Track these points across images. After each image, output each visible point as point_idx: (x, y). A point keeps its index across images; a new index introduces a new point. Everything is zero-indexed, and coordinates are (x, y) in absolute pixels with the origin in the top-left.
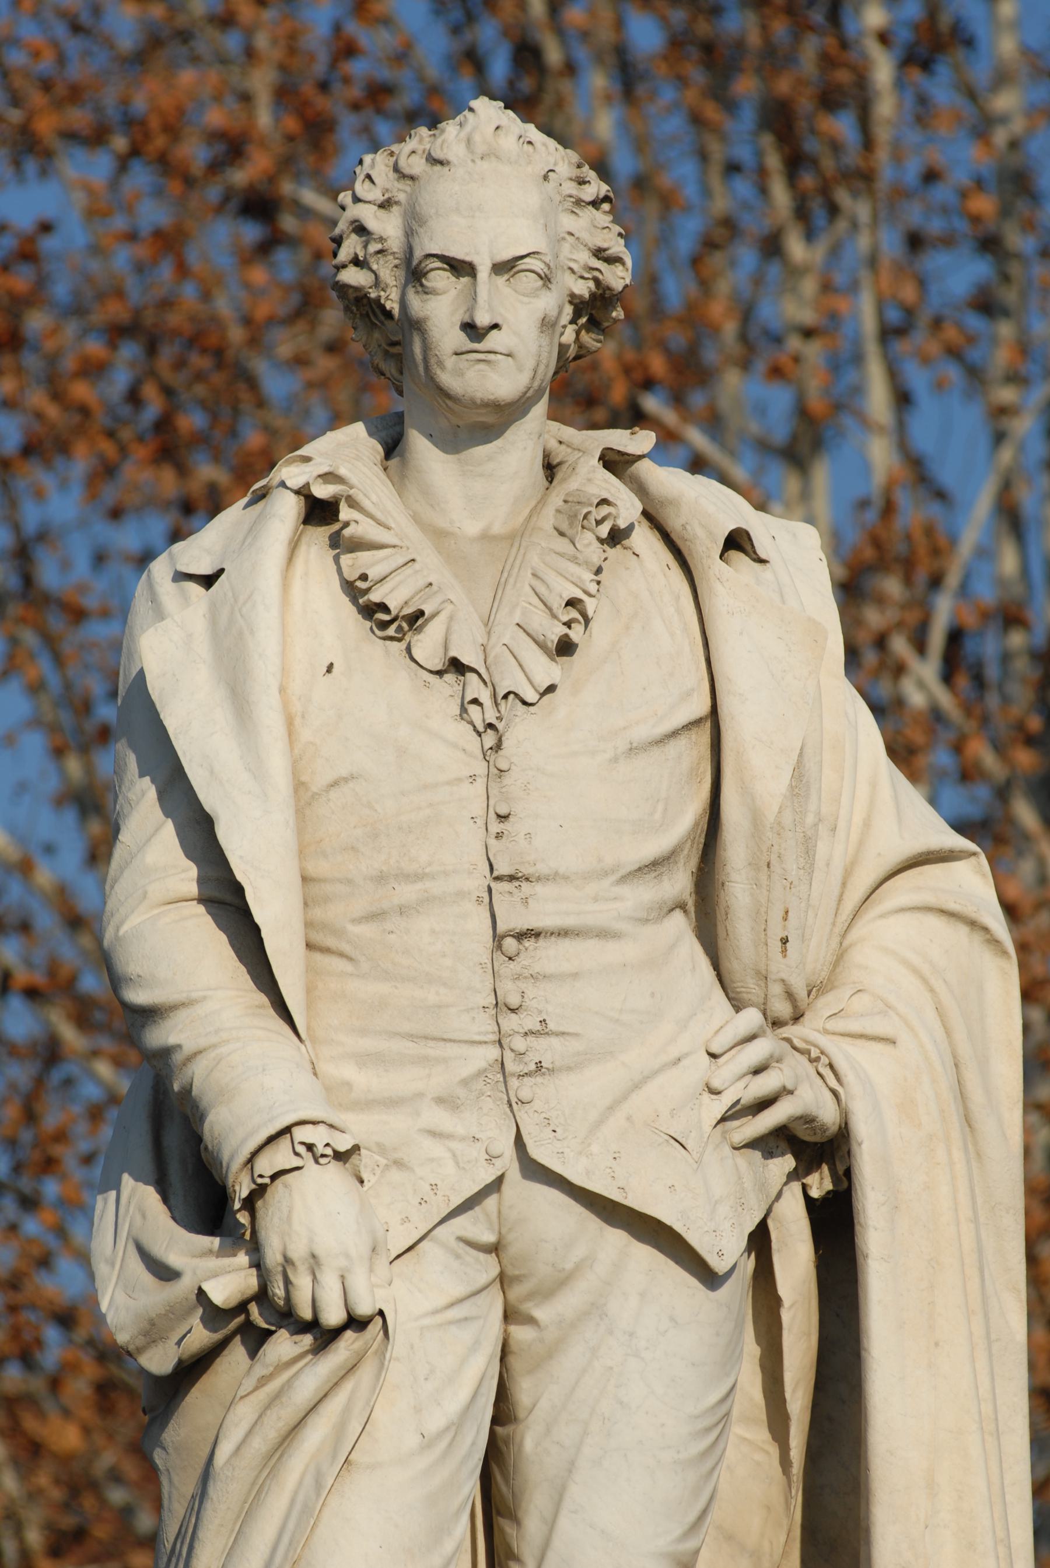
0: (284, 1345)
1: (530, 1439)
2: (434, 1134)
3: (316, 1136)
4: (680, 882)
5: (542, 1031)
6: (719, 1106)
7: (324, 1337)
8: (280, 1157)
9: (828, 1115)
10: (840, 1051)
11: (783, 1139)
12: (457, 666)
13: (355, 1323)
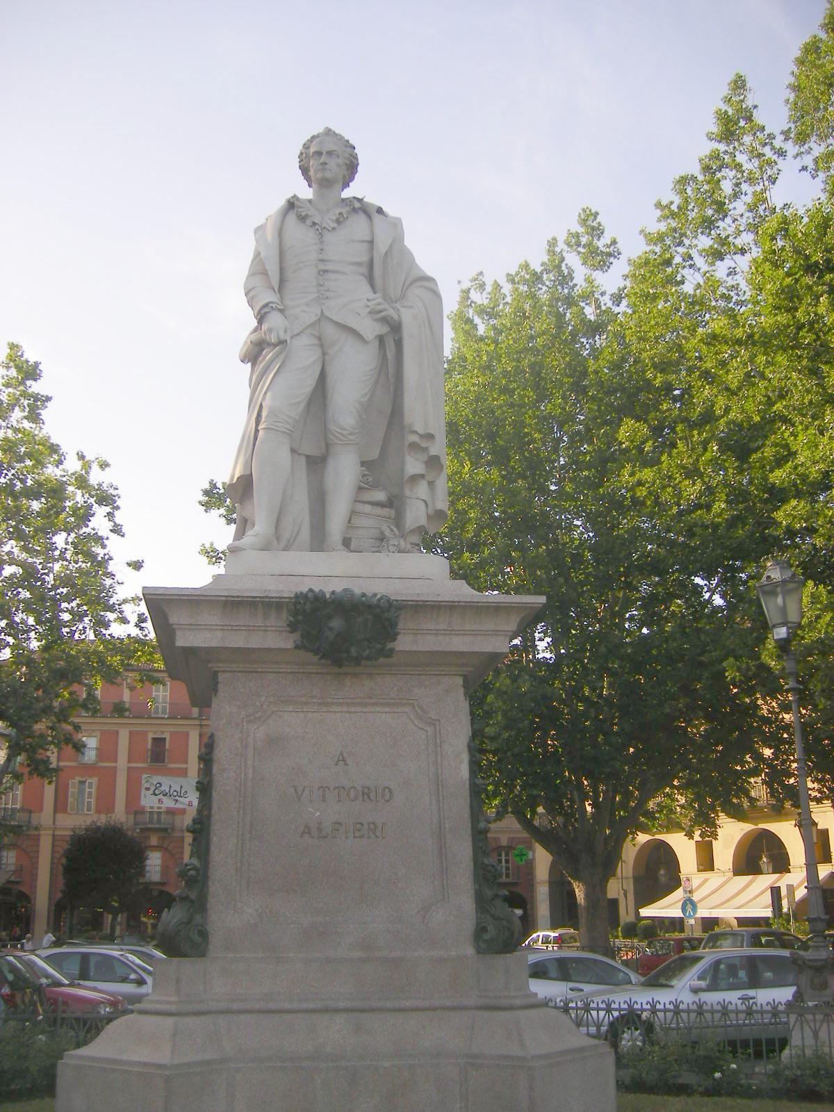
1: (330, 381)
2: (304, 311)
3: (274, 306)
4: (364, 270)
5: (328, 290)
6: (368, 310)
7: (275, 345)
8: (266, 310)
9: (396, 317)
10: (402, 310)
11: (385, 320)
12: (314, 224)
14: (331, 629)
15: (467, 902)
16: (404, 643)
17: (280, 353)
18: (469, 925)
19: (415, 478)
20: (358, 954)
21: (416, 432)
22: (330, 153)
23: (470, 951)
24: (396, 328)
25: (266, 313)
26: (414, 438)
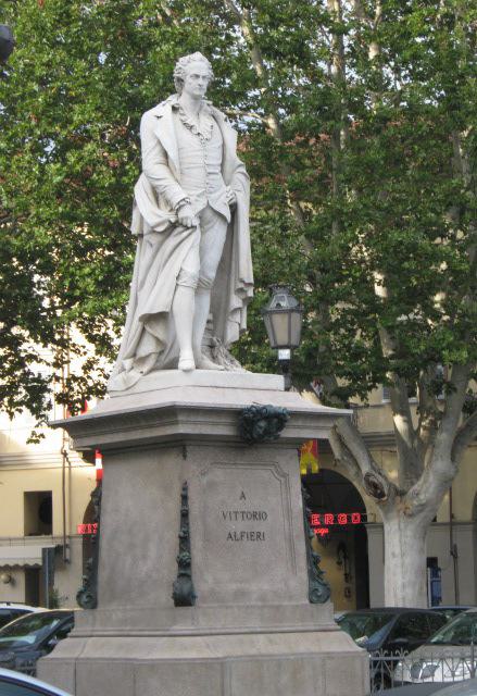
0: (180, 229)
7: (188, 228)
13: (192, 227)
14: (261, 428)
15: (304, 575)
16: (287, 433)
17: (190, 234)
18: (306, 589)
19: (236, 310)
20: (260, 604)
21: (243, 282)
22: (204, 77)
23: (307, 602)
24: (234, 208)
25: (183, 206)
26: (241, 285)
